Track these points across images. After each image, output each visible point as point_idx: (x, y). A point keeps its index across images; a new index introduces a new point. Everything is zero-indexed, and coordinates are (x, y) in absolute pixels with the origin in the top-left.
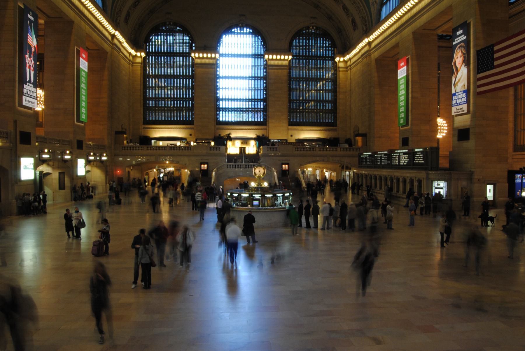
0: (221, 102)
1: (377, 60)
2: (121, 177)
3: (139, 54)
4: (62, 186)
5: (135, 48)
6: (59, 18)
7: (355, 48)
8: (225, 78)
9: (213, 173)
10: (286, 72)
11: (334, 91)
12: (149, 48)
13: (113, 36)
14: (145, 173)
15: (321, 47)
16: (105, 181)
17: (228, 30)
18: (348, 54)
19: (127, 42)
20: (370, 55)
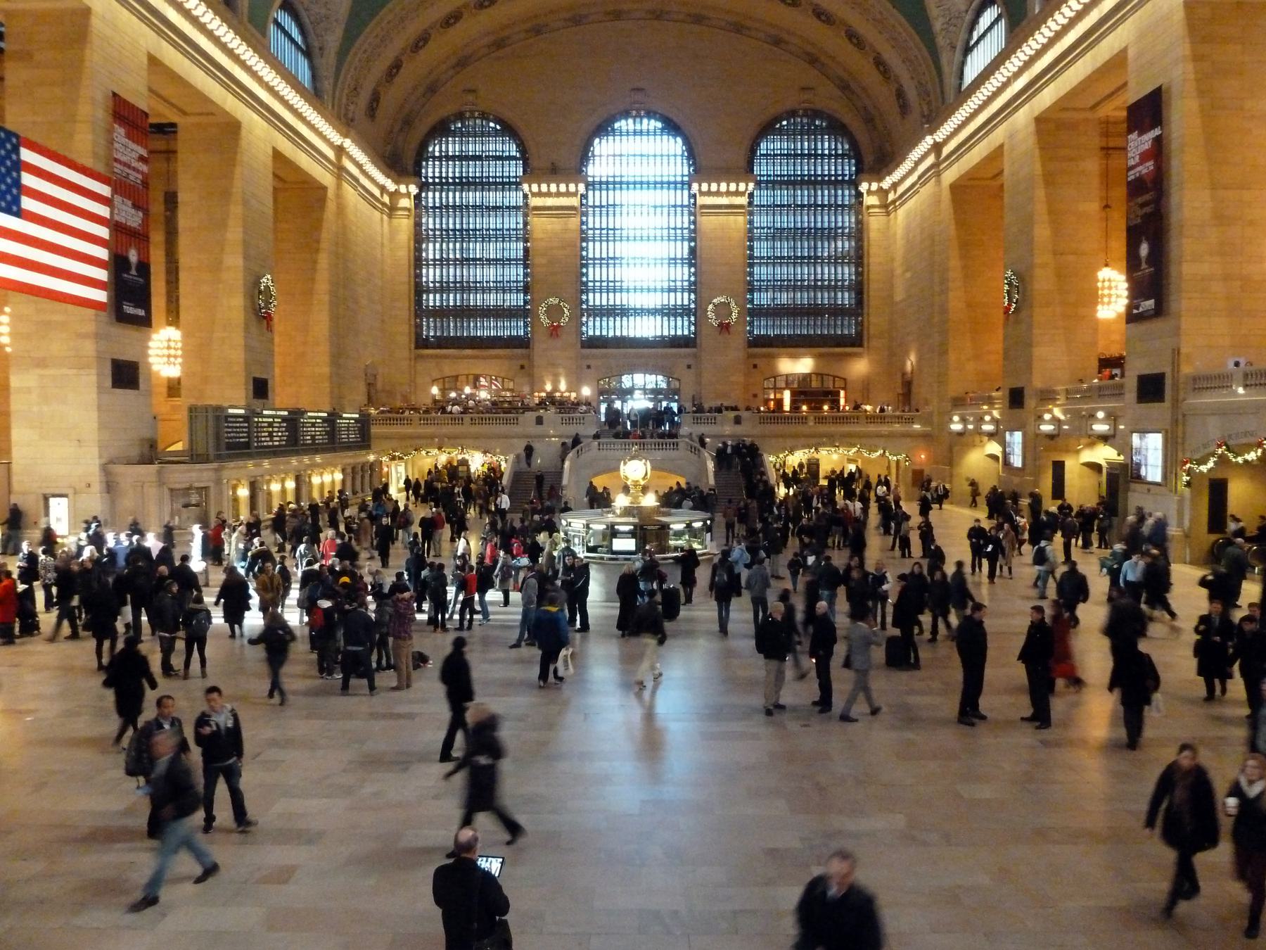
0: (591, 295)
1: (954, 187)
3: (403, 189)
7: (903, 159)
10: (740, 221)
11: (858, 258)
13: (340, 150)
17: (604, 128)
18: (889, 173)
19: (373, 162)
20: (938, 174)
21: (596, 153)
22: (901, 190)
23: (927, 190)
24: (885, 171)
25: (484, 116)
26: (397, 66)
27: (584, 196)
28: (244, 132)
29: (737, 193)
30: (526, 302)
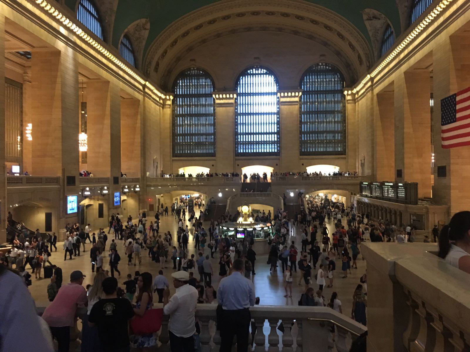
1: (377, 94)
2: (152, 203)
3: (168, 97)
4: (101, 215)
5: (164, 92)
6: (98, 79)
7: (360, 83)
8: (243, 114)
9: (228, 201)
10: (297, 107)
12: (177, 91)
13: (144, 86)
14: (174, 199)
15: (331, 82)
16: (138, 208)
17: (245, 74)
18: (355, 88)
20: (372, 90)
21: (241, 82)
22: (360, 94)
23: (369, 95)
24: (353, 87)
25: (198, 69)
26: (165, 52)
27: (236, 99)
28: (111, 85)
29: (295, 96)
30: (214, 139)
